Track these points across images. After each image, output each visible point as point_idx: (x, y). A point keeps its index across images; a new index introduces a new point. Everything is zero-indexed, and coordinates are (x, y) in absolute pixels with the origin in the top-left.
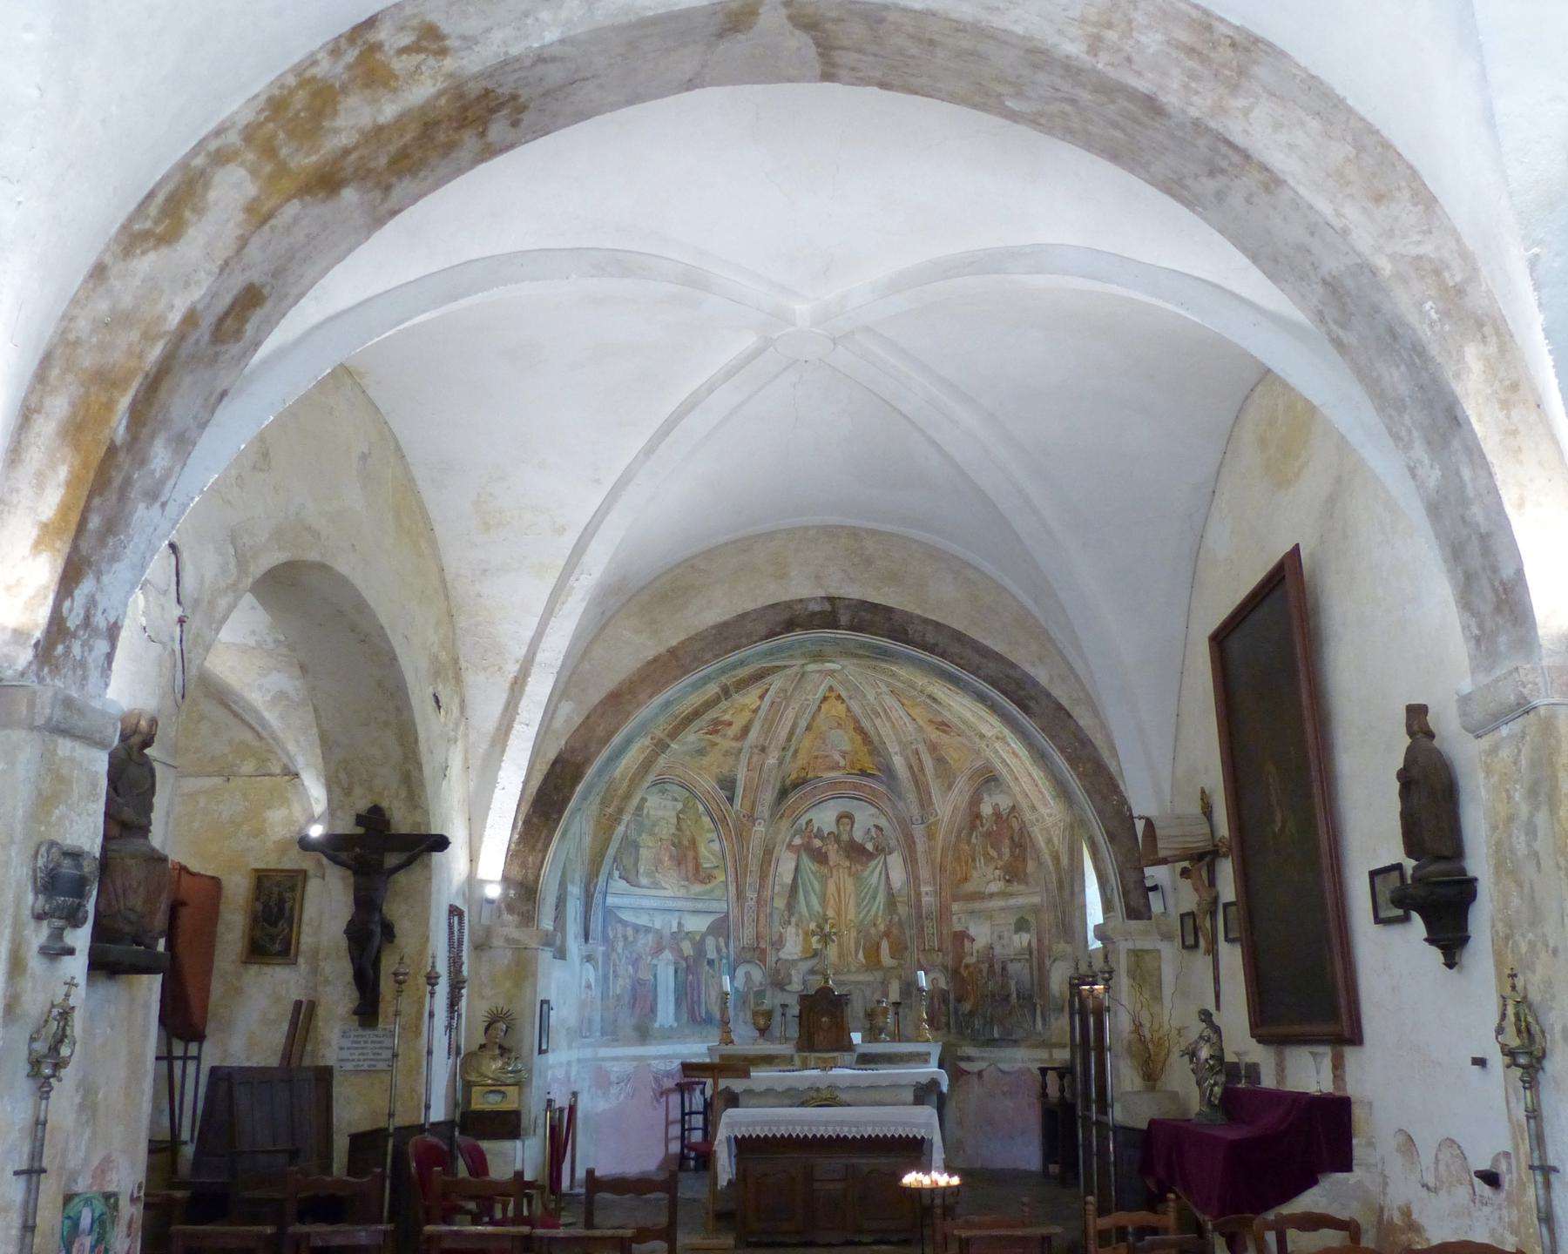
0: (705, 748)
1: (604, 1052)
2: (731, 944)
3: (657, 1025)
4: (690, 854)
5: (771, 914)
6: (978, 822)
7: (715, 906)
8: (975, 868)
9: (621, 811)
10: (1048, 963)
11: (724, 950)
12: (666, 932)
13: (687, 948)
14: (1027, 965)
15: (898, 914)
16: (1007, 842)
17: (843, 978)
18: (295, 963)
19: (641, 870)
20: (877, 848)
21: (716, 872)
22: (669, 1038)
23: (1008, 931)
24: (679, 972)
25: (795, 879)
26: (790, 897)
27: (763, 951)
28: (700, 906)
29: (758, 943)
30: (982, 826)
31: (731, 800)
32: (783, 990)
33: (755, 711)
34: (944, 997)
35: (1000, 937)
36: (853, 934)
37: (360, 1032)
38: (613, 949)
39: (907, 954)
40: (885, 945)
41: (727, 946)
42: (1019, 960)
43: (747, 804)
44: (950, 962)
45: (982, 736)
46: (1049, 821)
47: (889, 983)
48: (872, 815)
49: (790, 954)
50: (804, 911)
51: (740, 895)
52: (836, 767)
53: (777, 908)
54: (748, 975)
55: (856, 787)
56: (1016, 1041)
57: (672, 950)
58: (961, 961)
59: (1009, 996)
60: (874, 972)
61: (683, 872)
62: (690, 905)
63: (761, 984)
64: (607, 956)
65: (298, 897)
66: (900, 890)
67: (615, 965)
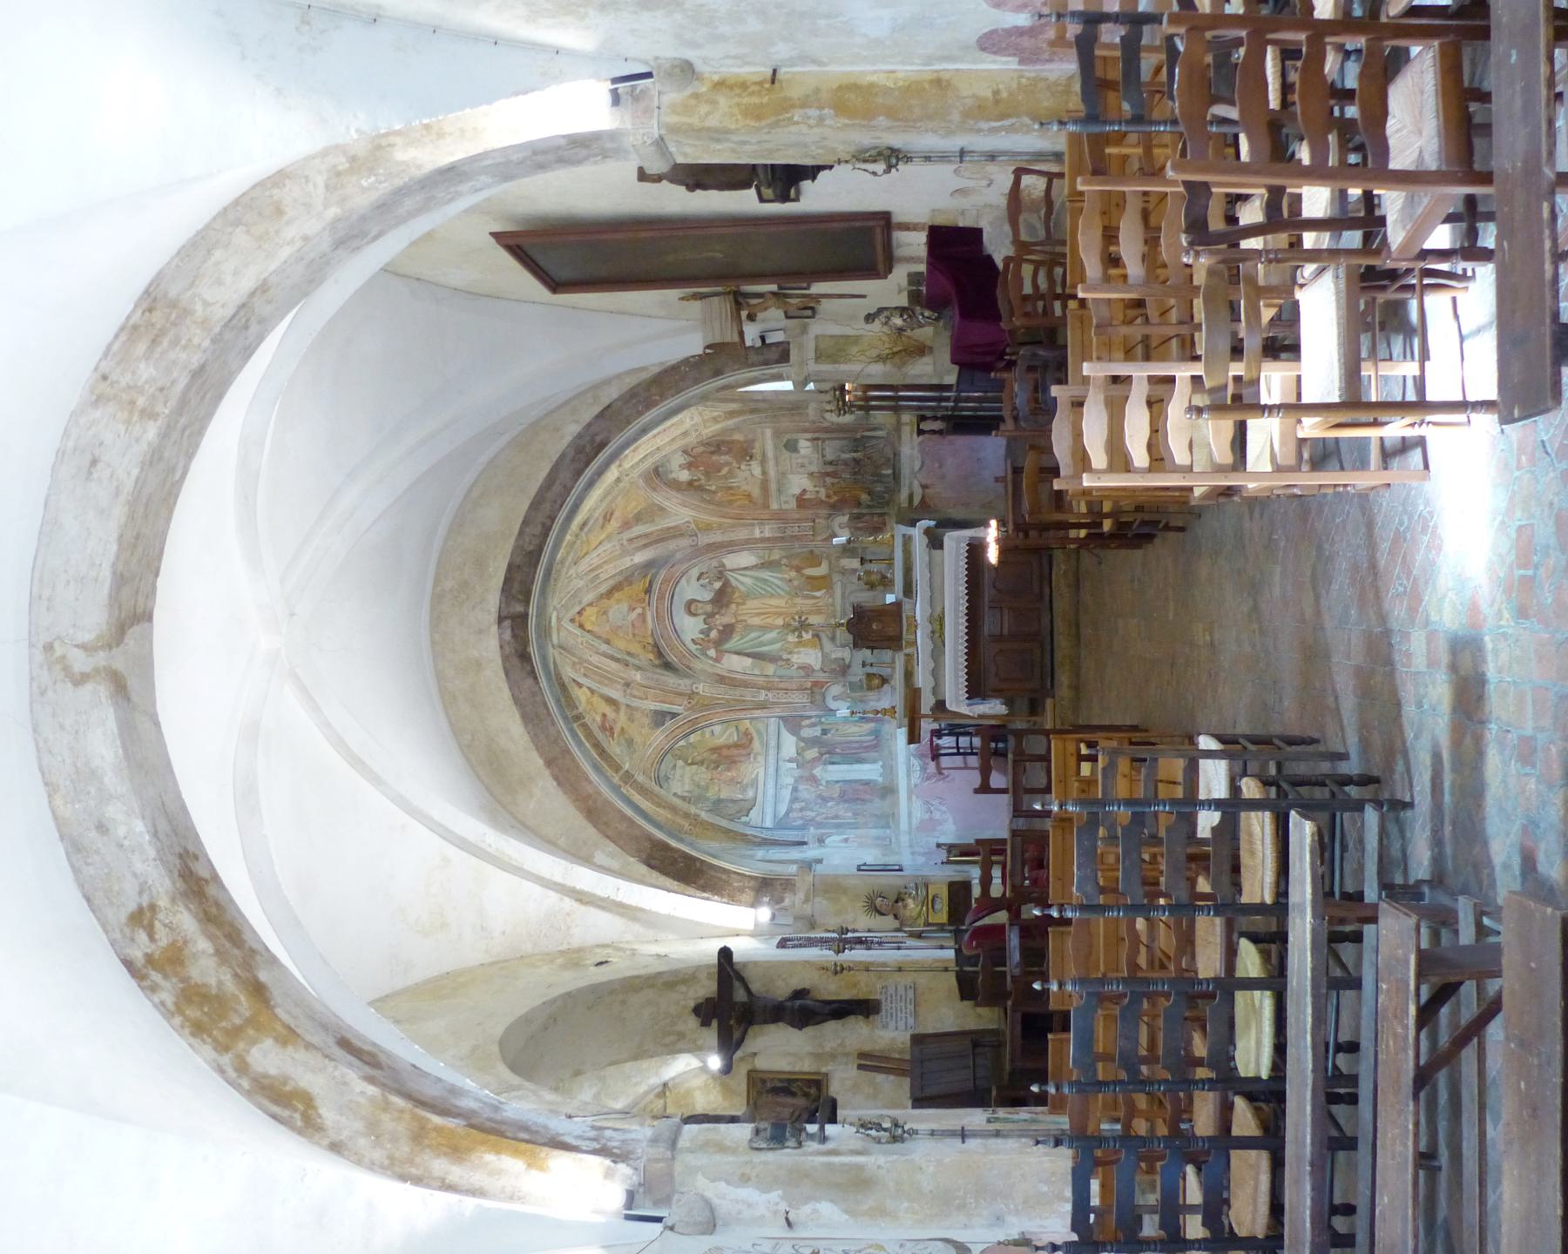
0: (626, 740)
1: (904, 825)
2: (808, 713)
3: (880, 780)
4: (725, 752)
5: (781, 677)
6: (696, 484)
7: (772, 728)
8: (738, 487)
9: (687, 815)
10: (826, 424)
11: (813, 720)
12: (797, 773)
13: (812, 753)
15: (780, 559)
16: (715, 458)
17: (838, 608)
18: (826, 1075)
19: (740, 796)
20: (719, 578)
21: (742, 729)
25: (748, 655)
28: (773, 743)
30: (699, 480)
31: (674, 715)
32: (849, 666)
33: (592, 691)
34: (856, 518)
35: (803, 466)
36: (799, 601)
37: (883, 1013)
38: (812, 820)
39: (817, 551)
40: (809, 572)
41: (809, 717)
43: (678, 700)
44: (824, 512)
45: (618, 480)
46: (697, 419)
48: (688, 582)
50: (778, 646)
51: (762, 706)
52: (643, 616)
54: (835, 698)
55: (661, 597)
57: (813, 768)
58: (822, 501)
59: (854, 459)
61: (742, 759)
62: (772, 752)
64: (819, 825)
65: (771, 1076)
66: (759, 557)
67: (826, 818)
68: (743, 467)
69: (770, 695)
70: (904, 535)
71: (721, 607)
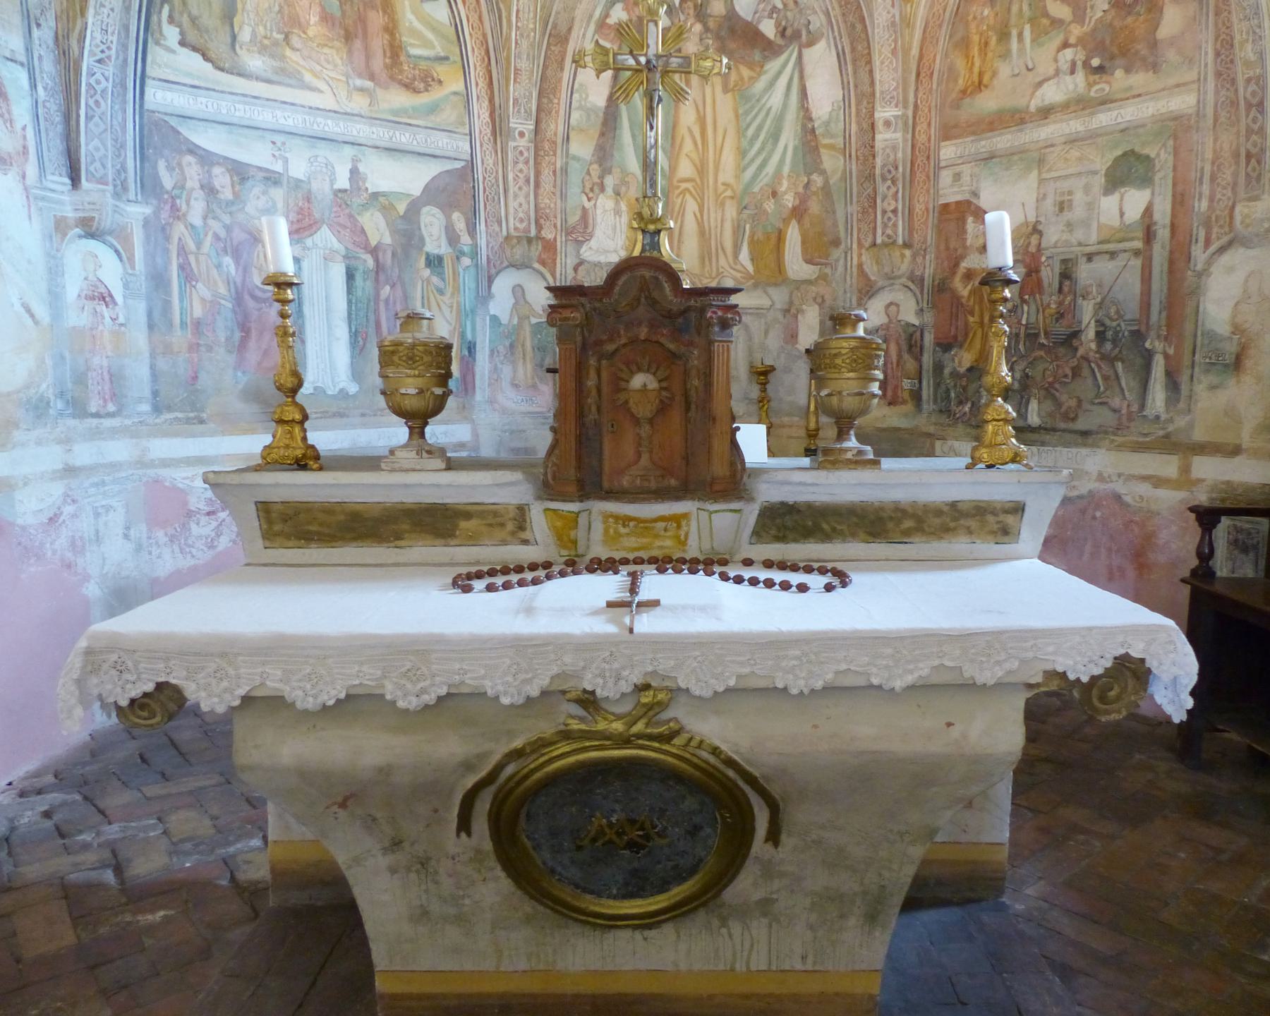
1: (162, 447)
2: (482, 227)
5: (565, 171)
7: (442, 142)
8: (1006, 55)
10: (1199, 255)
11: (465, 239)
12: (321, 188)
13: (377, 228)
14: (1137, 263)
15: (823, 172)
19: (245, 35)
20: (782, 33)
21: (440, 70)
22: (341, 415)
23: (1087, 189)
24: (359, 281)
26: (602, 134)
27: (550, 247)
28: (403, 138)
29: (539, 227)
34: (912, 341)
35: (1062, 207)
36: (731, 211)
39: (837, 253)
40: (793, 236)
41: (472, 230)
42: (1113, 255)
44: (929, 268)
47: (799, 311)
51: (498, 127)
53: (576, 158)
54: (518, 291)
56: (1085, 434)
57: (337, 228)
58: (957, 265)
59: (1076, 334)
60: (771, 290)
61: (359, 57)
62: (380, 134)
64: (158, 231)
66: (827, 123)
67: (182, 251)
68: (1068, 54)
69: (523, 143)
70: (1018, 509)
71: (718, 37)
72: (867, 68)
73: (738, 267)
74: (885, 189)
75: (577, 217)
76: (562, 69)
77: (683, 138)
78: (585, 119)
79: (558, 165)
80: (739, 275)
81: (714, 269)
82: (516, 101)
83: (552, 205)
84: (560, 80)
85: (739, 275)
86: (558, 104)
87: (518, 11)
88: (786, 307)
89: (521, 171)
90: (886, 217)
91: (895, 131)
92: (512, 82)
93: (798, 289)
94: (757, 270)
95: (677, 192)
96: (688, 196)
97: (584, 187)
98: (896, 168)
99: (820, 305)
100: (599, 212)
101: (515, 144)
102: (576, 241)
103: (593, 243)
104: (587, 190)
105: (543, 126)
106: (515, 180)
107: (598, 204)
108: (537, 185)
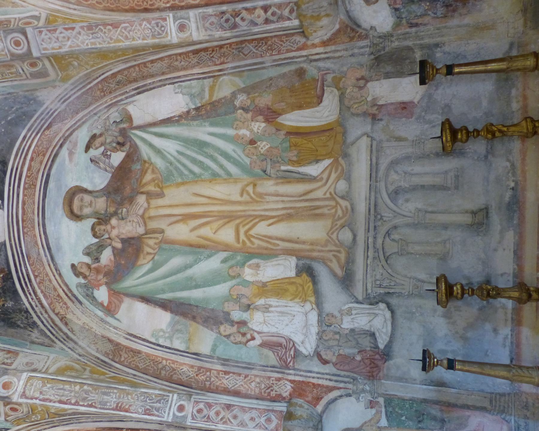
5: (225, 361)
15: (234, 95)
17: (362, 207)
25: (164, 305)
26: (194, 318)
39: (312, 71)
47: (374, 104)
48: (71, 154)
49: (306, 326)
53: (214, 348)
60: (350, 138)
63: (372, 404)
66: (192, 96)
69: (189, 408)
71: (121, 204)
72: (149, 65)
73: (325, 176)
74: (245, 23)
75: (270, 353)
76: (139, 352)
77: (199, 237)
78: (180, 335)
79: (220, 368)
80: (333, 176)
81: (327, 203)
82: (147, 412)
83: (258, 380)
84: (148, 355)
85: (333, 176)
86: (167, 360)
87: (60, 402)
88: (369, 120)
89: (217, 413)
90: (272, 18)
91: (188, 19)
92: (128, 414)
93: (349, 108)
94: (328, 155)
95: (248, 244)
96: (252, 232)
97: (240, 343)
98: (223, 13)
99: (367, 81)
100: (265, 329)
101: (189, 419)
102: (294, 357)
103: (297, 339)
104: (244, 340)
105: (184, 378)
106: (225, 423)
107: (257, 329)
108: (237, 394)
